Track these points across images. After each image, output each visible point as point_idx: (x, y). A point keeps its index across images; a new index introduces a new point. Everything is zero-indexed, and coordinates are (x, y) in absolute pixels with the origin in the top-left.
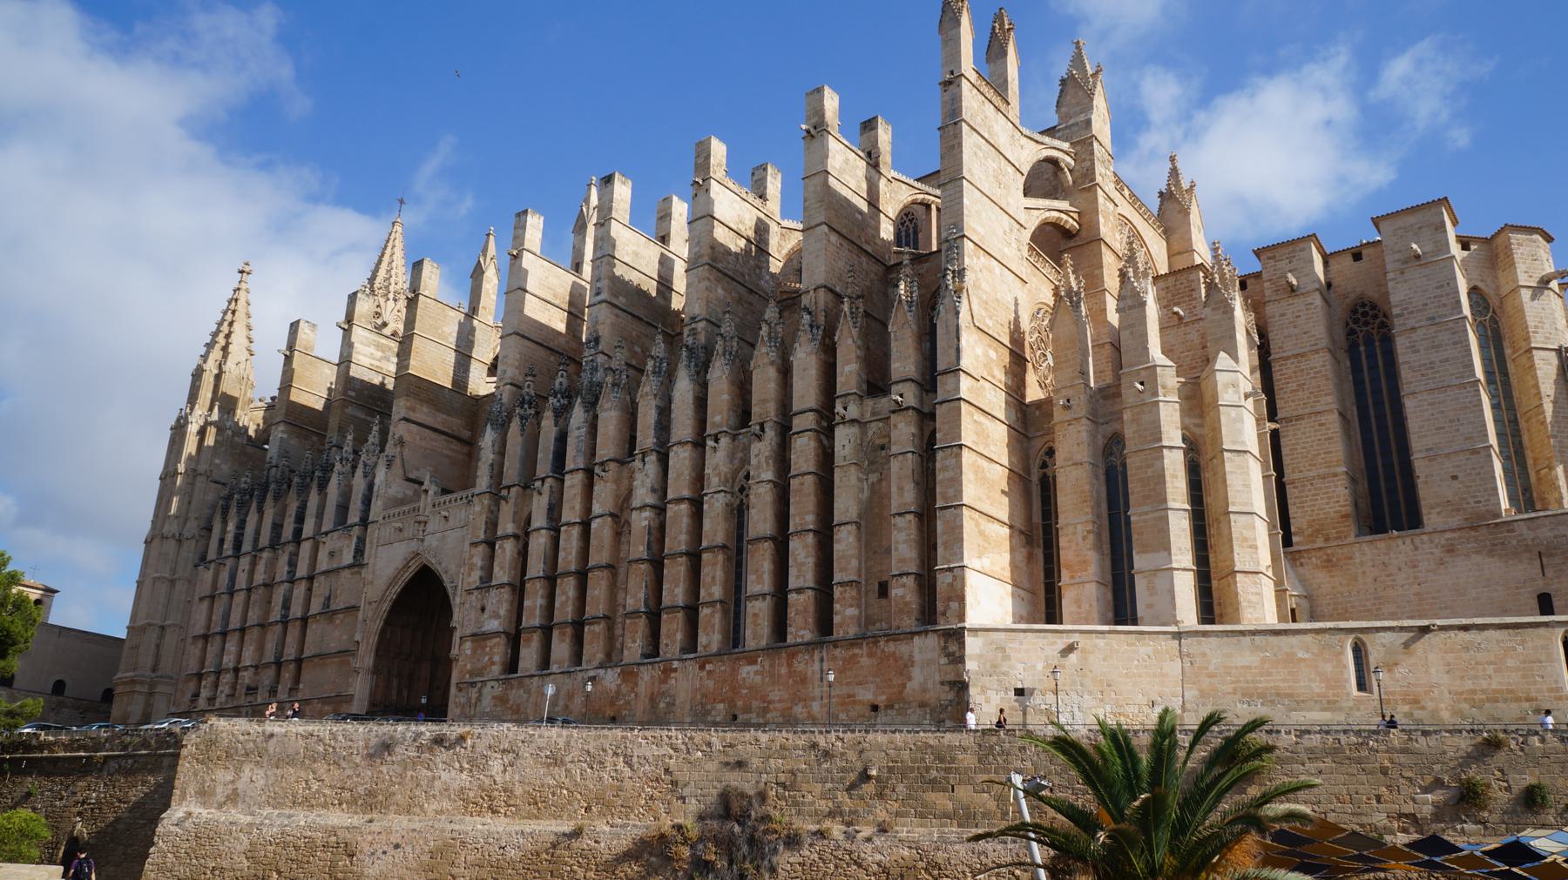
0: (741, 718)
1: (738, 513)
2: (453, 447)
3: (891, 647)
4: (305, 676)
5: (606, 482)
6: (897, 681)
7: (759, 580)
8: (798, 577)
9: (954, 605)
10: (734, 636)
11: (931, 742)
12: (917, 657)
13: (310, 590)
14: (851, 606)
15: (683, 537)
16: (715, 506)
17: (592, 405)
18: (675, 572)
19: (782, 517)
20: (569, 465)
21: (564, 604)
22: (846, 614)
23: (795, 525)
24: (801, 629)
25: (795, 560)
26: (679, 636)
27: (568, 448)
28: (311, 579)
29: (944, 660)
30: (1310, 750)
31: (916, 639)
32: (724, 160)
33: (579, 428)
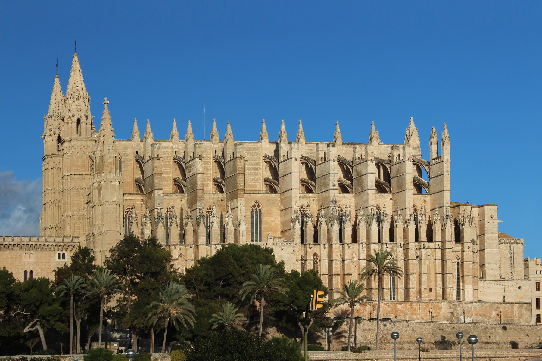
0: (398, 318)
3: (437, 304)
5: (350, 250)
6: (438, 311)
8: (412, 285)
9: (451, 296)
10: (393, 296)
11: (468, 326)
12: (443, 307)
14: (427, 293)
21: (336, 283)
22: (426, 295)
23: (411, 272)
25: (411, 281)
27: (333, 237)
29: (449, 308)
30: (511, 328)
33: (337, 231)
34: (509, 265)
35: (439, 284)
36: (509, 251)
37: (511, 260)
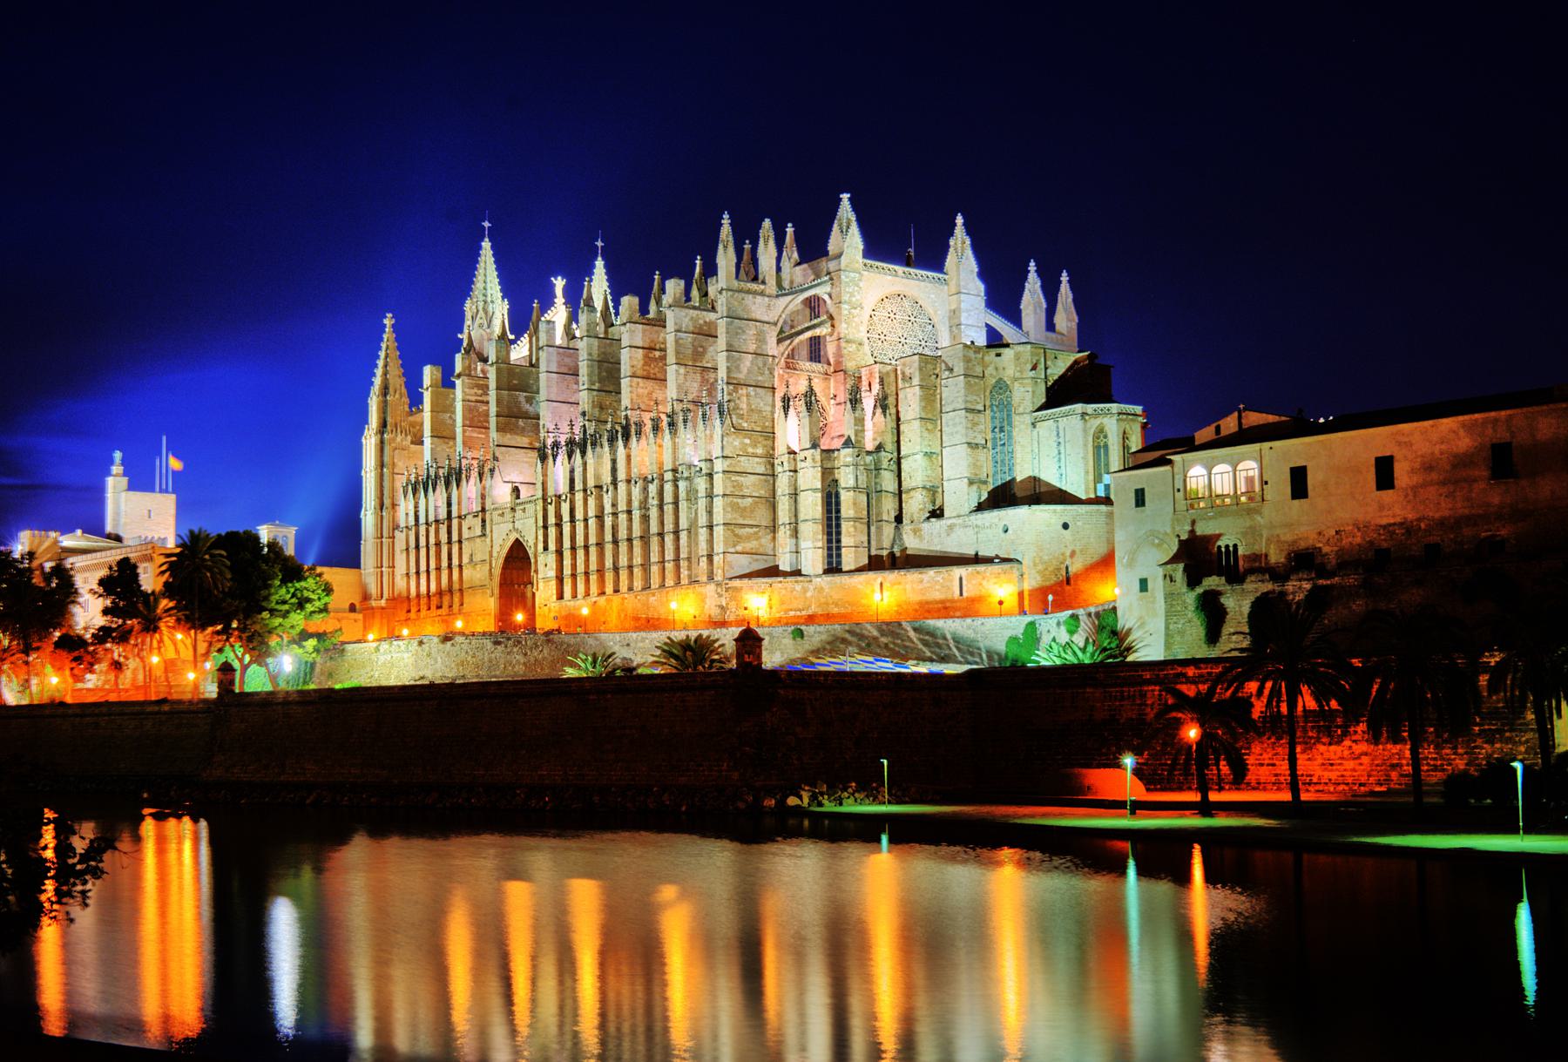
1: (645, 519)
2: (529, 455)
4: (466, 600)
7: (655, 557)
12: (708, 594)
13: (460, 549)
15: (625, 532)
16: (636, 514)
17: (583, 453)
18: (623, 547)
19: (662, 523)
20: (577, 488)
21: (580, 564)
22: (684, 573)
24: (670, 582)
26: (626, 583)
28: (460, 542)
29: (716, 596)
30: (819, 632)
31: (708, 586)
32: (638, 308)
34: (1055, 471)
35: (702, 550)
36: (1056, 438)
37: (1059, 460)
